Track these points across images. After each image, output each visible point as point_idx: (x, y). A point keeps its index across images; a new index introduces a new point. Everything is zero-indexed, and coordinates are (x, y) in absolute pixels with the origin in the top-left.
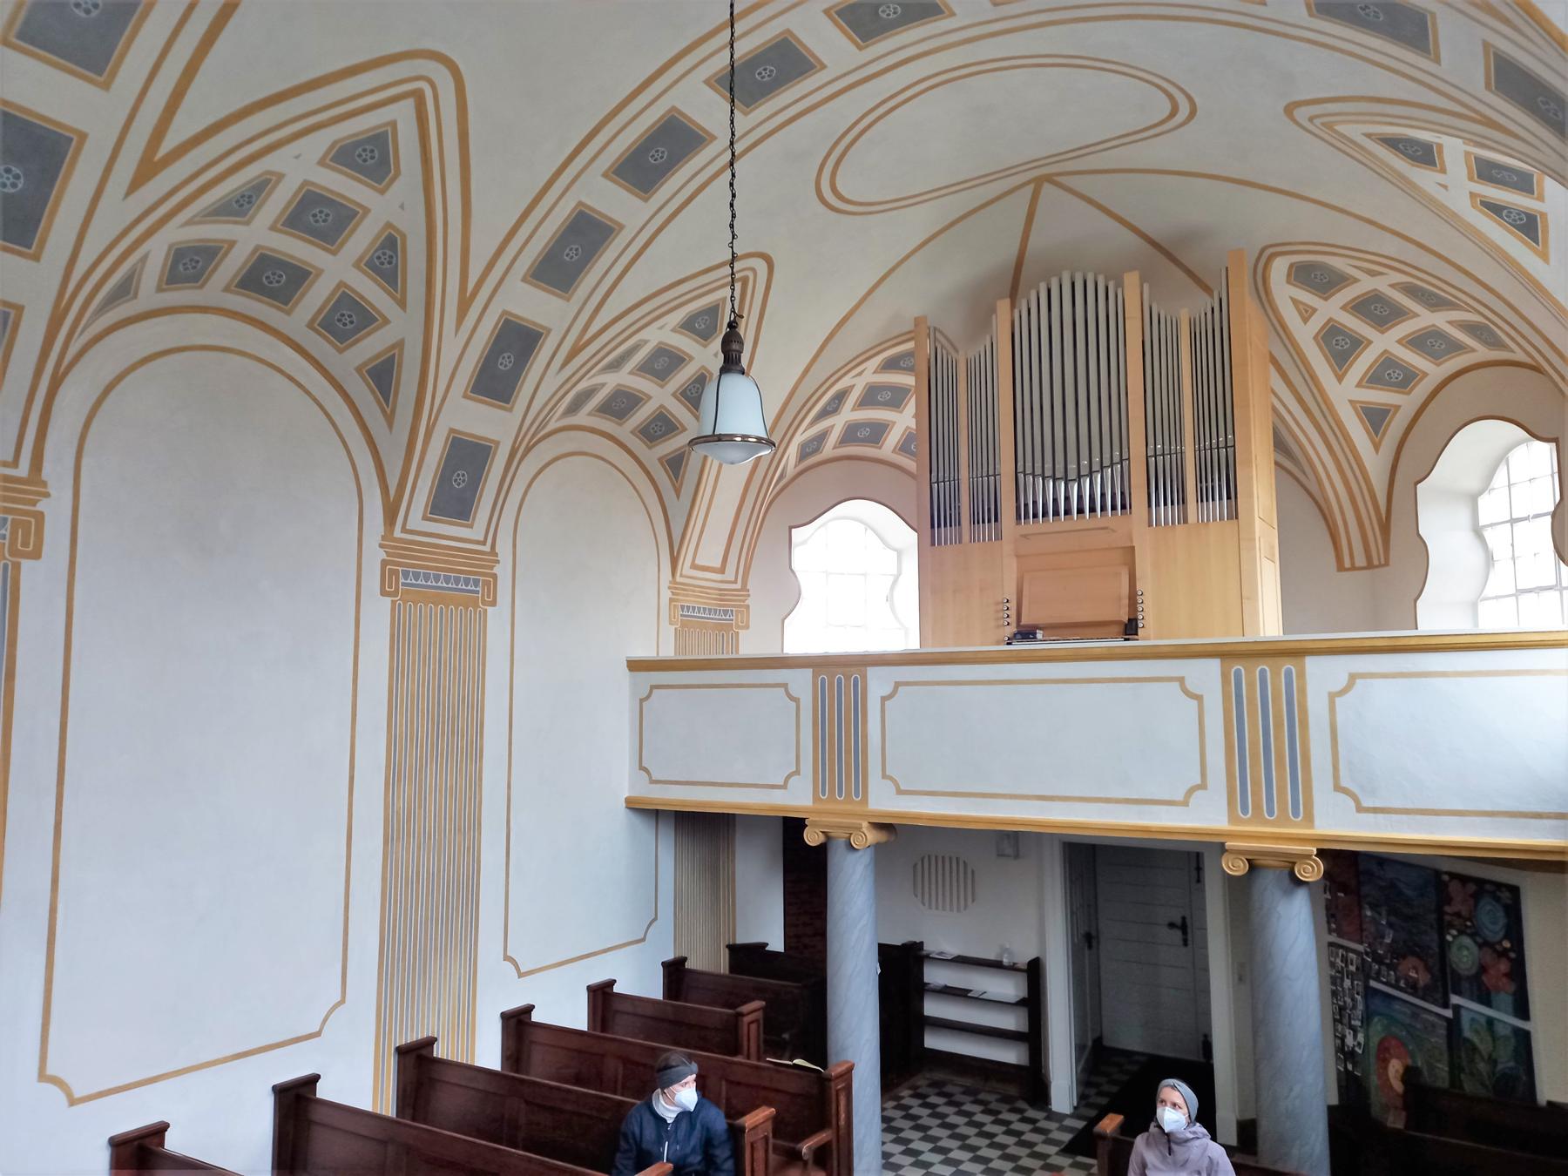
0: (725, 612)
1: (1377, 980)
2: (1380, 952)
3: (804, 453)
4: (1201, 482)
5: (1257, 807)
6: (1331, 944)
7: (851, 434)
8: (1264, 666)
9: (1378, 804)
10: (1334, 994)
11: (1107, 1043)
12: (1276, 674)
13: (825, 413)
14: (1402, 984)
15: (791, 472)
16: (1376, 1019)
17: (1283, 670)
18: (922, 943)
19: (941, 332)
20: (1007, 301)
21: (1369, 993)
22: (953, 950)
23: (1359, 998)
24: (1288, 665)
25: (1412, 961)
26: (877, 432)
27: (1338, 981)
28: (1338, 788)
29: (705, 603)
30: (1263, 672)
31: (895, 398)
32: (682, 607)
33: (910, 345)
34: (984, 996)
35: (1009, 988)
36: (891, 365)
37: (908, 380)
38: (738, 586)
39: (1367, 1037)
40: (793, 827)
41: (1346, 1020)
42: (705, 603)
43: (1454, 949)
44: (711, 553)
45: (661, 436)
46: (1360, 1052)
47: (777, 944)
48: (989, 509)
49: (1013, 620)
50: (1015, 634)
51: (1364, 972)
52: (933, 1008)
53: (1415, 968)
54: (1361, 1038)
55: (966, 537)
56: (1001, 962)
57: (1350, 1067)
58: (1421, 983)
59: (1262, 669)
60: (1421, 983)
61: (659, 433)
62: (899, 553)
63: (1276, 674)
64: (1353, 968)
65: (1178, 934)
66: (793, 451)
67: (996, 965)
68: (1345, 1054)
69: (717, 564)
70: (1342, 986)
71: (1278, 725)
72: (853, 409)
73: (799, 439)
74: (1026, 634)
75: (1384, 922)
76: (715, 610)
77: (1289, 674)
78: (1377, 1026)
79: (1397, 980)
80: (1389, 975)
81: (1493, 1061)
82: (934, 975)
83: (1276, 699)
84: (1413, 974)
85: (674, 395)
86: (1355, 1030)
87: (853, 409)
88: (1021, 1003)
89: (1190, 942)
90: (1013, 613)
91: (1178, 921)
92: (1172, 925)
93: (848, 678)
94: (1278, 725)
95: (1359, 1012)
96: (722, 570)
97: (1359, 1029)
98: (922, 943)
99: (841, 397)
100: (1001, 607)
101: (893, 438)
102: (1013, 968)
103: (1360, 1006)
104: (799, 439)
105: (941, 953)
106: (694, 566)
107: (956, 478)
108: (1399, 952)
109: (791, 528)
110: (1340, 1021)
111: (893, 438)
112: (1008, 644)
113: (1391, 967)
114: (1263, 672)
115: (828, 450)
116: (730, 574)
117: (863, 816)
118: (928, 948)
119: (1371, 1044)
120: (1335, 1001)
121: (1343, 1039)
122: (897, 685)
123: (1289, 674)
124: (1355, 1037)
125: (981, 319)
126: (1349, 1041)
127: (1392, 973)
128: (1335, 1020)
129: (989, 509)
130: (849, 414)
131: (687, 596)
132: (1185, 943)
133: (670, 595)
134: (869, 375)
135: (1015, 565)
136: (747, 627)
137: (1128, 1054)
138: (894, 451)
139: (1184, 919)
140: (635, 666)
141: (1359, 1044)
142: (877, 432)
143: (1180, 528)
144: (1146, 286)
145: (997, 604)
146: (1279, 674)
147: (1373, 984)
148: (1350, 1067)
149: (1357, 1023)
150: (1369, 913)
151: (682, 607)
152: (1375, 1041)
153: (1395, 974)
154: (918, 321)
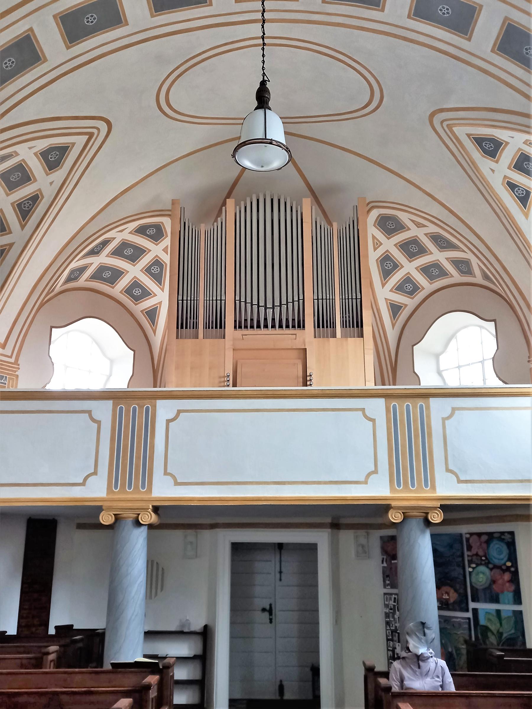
10: (388, 623)
12: (415, 407)
17: (419, 405)
27: (391, 614)
48: (212, 321)
59: (407, 404)
63: (415, 407)
65: (267, 614)
70: (393, 617)
83: (415, 421)
89: (273, 621)
92: (264, 610)
99: (105, 243)
100: (223, 379)
120: (388, 628)
122: (179, 412)
123: (421, 407)
129: (212, 321)
139: (271, 605)
145: (220, 377)
146: (417, 407)
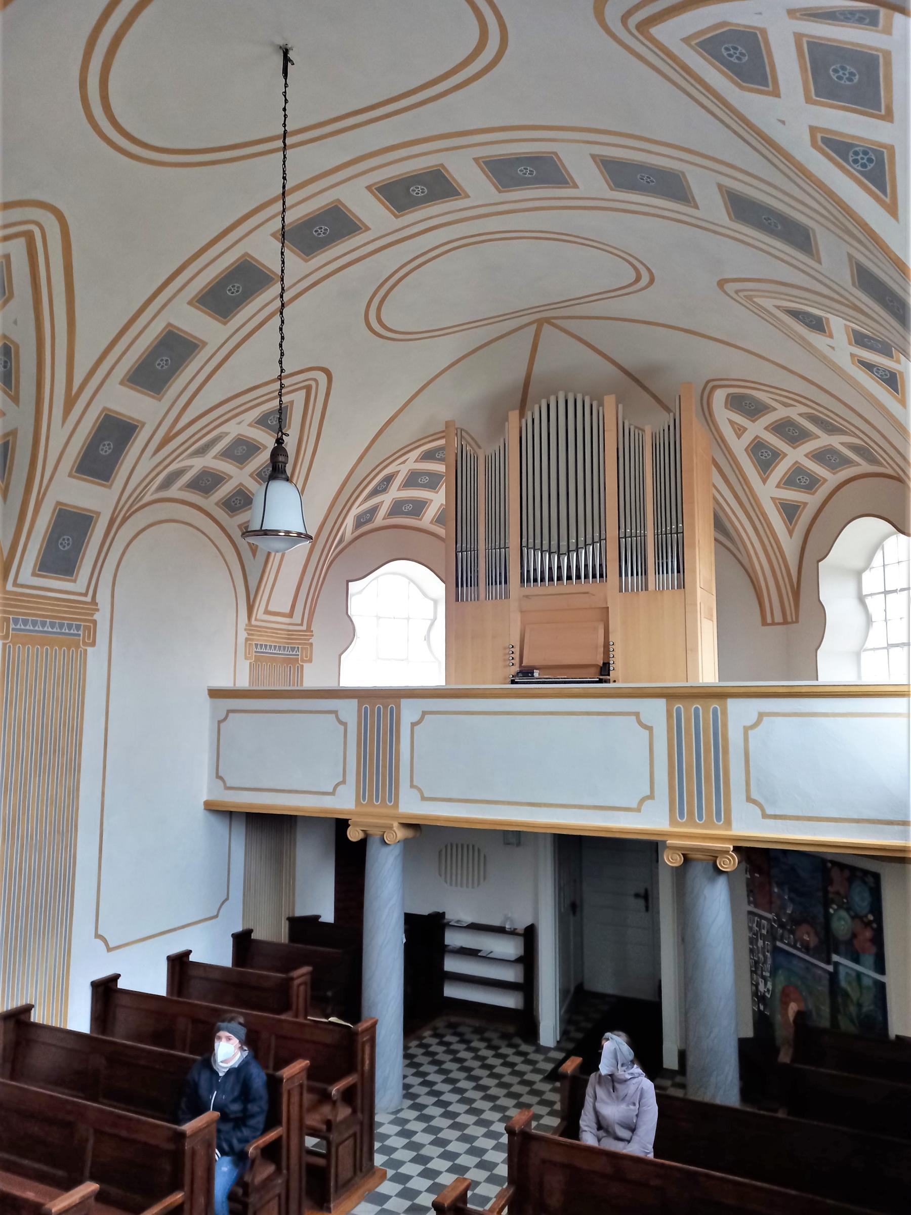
0: (293, 649)
1: (782, 941)
2: (784, 920)
3: (360, 521)
4: (658, 559)
5: (691, 813)
6: (750, 913)
7: (397, 508)
8: (697, 705)
9: (778, 812)
10: (751, 951)
11: (588, 986)
12: (706, 711)
13: (375, 492)
14: (798, 945)
15: (348, 536)
16: (780, 972)
18: (444, 914)
19: (464, 430)
20: (517, 412)
21: (776, 950)
22: (468, 919)
23: (768, 954)
24: (715, 705)
25: (805, 927)
26: (418, 507)
27: (754, 941)
28: (749, 799)
29: (273, 642)
30: (697, 709)
31: (433, 482)
32: (256, 645)
33: (442, 442)
34: (490, 956)
35: (509, 948)
36: (428, 456)
37: (440, 468)
38: (304, 628)
39: (774, 985)
40: (342, 825)
41: (759, 972)
42: (273, 642)
43: (835, 919)
44: (281, 600)
45: (241, 508)
46: (769, 996)
47: (328, 915)
48: (500, 574)
49: (517, 661)
50: (518, 673)
51: (772, 936)
52: (451, 965)
53: (808, 934)
54: (769, 985)
55: (482, 596)
56: (504, 928)
57: (762, 1008)
58: (812, 945)
60: (812, 945)
61: (238, 505)
62: (436, 602)
63: (706, 711)
64: (764, 932)
65: (641, 903)
66: (350, 521)
67: (499, 930)
68: (759, 997)
69: (287, 610)
70: (757, 945)
71: (707, 751)
72: (399, 489)
73: (355, 511)
74: (526, 673)
75: (786, 897)
76: (284, 648)
77: (715, 712)
78: (781, 978)
79: (795, 942)
80: (789, 938)
81: (860, 1006)
82: (453, 939)
84: (806, 937)
85: (251, 475)
86: (764, 978)
87: (399, 489)
88: (519, 960)
90: (517, 656)
91: (642, 892)
93: (385, 707)
94: (707, 751)
95: (768, 966)
96: (291, 615)
97: (769, 978)
98: (444, 914)
99: (389, 479)
101: (431, 512)
102: (513, 933)
103: (769, 961)
104: (355, 511)
105: (458, 921)
106: (267, 612)
107: (476, 549)
108: (796, 921)
109: (348, 582)
110: (756, 974)
111: (431, 512)
112: (513, 682)
113: (792, 932)
114: (697, 709)
115: (380, 519)
116: (297, 618)
117: (395, 818)
118: (449, 917)
119: (777, 990)
120: (752, 957)
121: (757, 986)
122: (424, 713)
123: (715, 712)
124: (766, 984)
125: (497, 425)
126: (762, 988)
127: (792, 936)
128: (752, 972)
129: (500, 574)
130: (395, 493)
131: (261, 636)
132: (647, 909)
133: (246, 635)
134: (411, 463)
135: (519, 619)
136: (310, 661)
137: (602, 996)
138: (431, 522)
140: (215, 693)
141: (768, 990)
142: (418, 507)
143: (643, 594)
144: (620, 406)
145: (505, 648)
147: (779, 944)
148: (762, 1008)
149: (767, 974)
150: (776, 890)
151: (256, 645)
152: (779, 987)
153: (794, 937)
154: (448, 424)
